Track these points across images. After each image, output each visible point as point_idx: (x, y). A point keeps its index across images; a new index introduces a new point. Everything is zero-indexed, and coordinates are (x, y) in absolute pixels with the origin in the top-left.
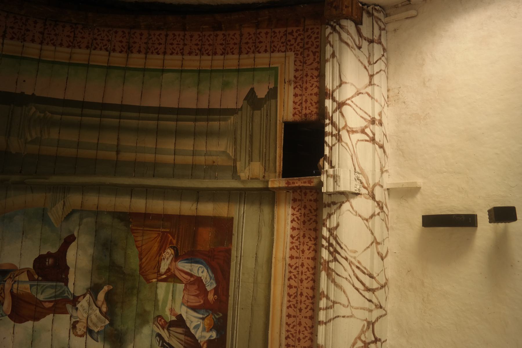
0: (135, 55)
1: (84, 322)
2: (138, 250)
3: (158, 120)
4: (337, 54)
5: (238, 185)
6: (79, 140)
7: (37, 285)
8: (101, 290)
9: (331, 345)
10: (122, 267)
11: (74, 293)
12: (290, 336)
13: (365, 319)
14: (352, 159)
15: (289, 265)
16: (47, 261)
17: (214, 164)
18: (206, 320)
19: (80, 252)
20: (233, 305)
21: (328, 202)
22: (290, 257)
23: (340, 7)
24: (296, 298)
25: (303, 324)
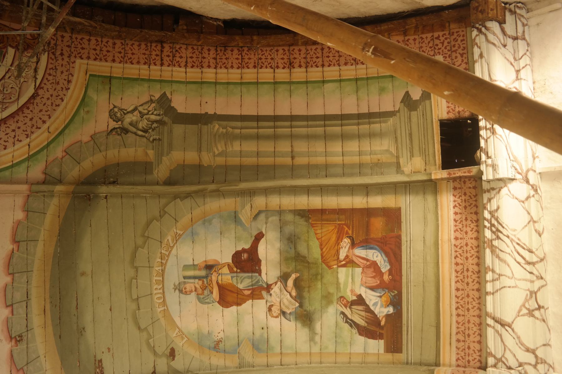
0: (297, 69)
2: (319, 242)
3: (325, 126)
4: (485, 54)
5: (405, 179)
6: (258, 149)
7: (237, 276)
8: (290, 278)
9: (499, 312)
10: (306, 257)
12: (460, 307)
13: (528, 289)
14: (507, 148)
15: (455, 245)
16: (243, 255)
17: (379, 162)
18: (383, 298)
19: (269, 247)
20: (406, 284)
21: (487, 189)
22: (454, 239)
23: (486, 11)
24: (463, 273)
25: (471, 296)
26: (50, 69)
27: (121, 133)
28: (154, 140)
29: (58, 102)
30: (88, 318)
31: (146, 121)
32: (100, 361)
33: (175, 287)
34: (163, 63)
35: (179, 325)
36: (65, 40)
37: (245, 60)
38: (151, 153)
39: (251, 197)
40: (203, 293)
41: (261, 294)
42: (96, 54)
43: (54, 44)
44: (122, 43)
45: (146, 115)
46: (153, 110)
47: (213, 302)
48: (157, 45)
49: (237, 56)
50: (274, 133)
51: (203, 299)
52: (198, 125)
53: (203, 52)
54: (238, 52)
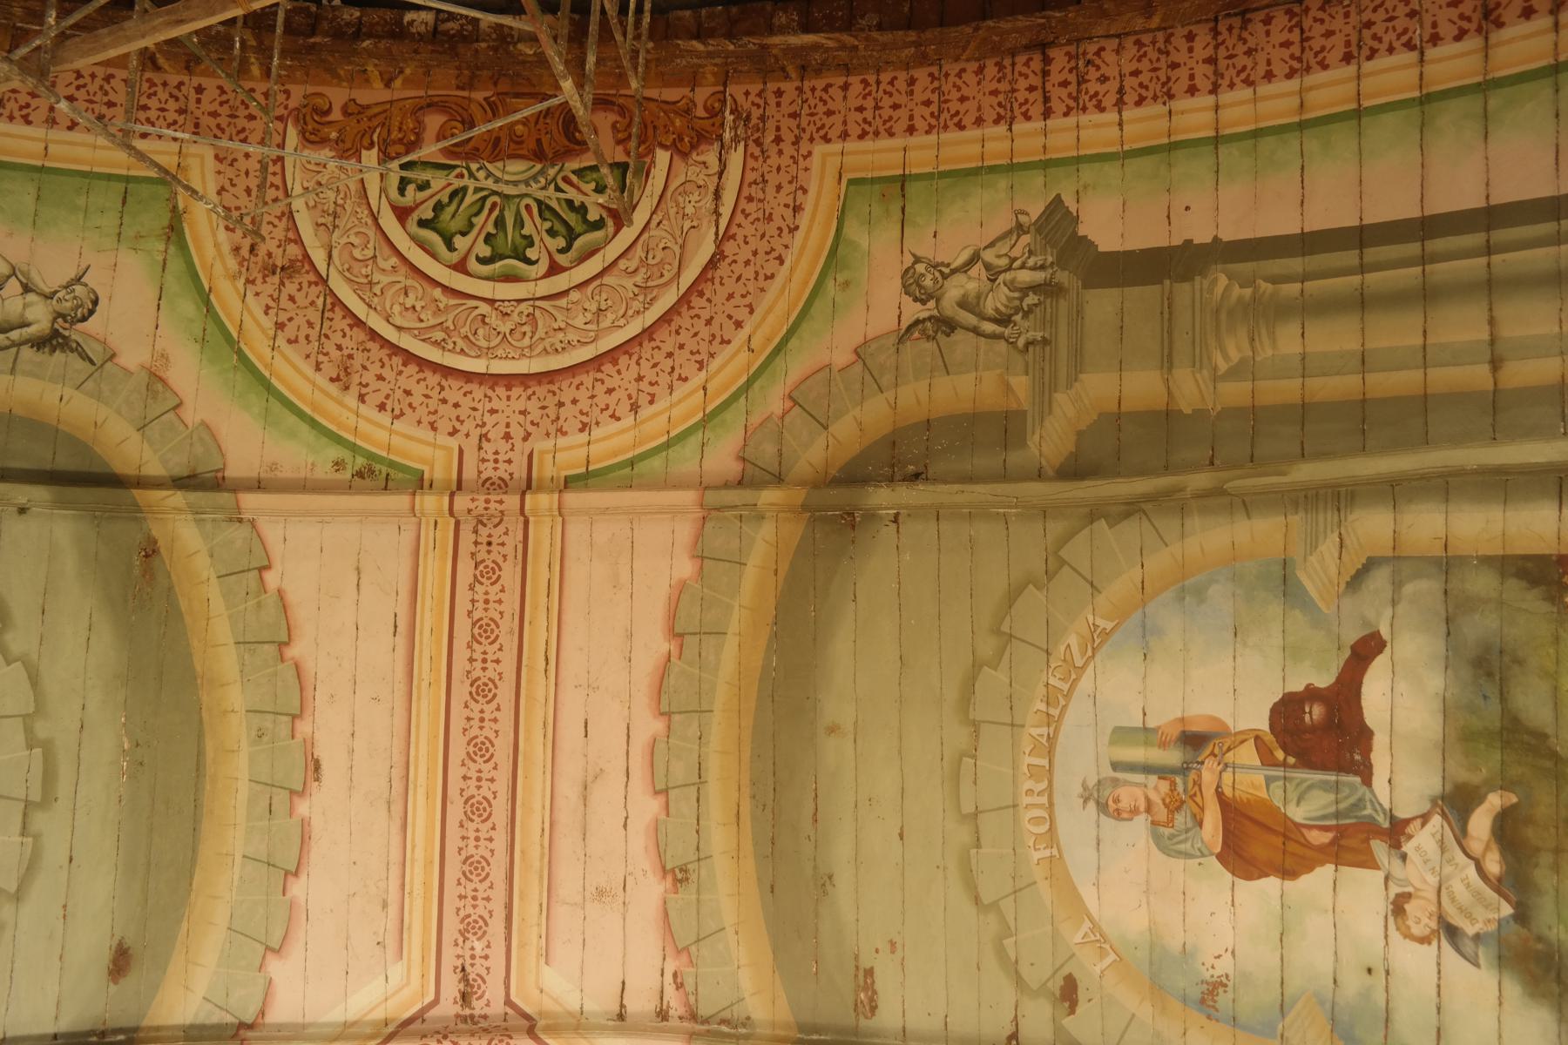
1: (1429, 901)
7: (1285, 778)
10: (1545, 736)
11: (1391, 810)
16: (1307, 710)
19: (1402, 686)
26: (750, 185)
27: (936, 332)
28: (1028, 344)
29: (773, 265)
30: (841, 851)
31: (1006, 290)
32: (870, 972)
33: (1087, 794)
34: (1050, 107)
35: (1091, 911)
36: (785, 100)
37: (1311, 43)
38: (1021, 384)
39: (1339, 510)
40: (1170, 823)
41: (1369, 852)
42: (865, 120)
43: (758, 119)
44: (931, 75)
45: (1005, 271)
46: (1024, 254)
47: (1203, 855)
48: (1031, 59)
49: (1285, 36)
50: (1420, 279)
51: (1169, 838)
52: (1162, 283)
53: (1170, 48)
54: (1290, 21)
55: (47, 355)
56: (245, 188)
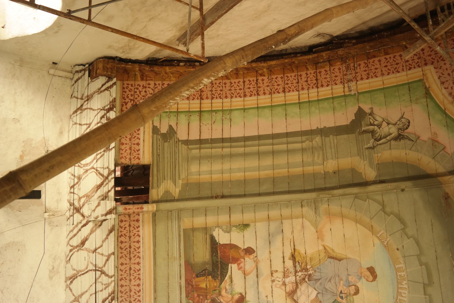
55: (399, 142)
56: (447, 74)
